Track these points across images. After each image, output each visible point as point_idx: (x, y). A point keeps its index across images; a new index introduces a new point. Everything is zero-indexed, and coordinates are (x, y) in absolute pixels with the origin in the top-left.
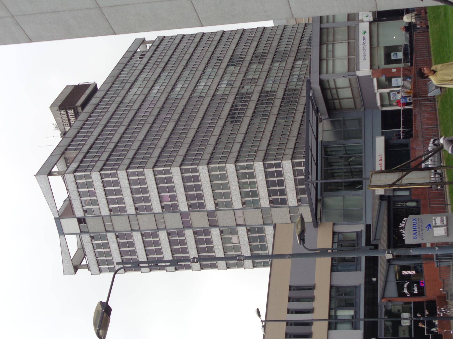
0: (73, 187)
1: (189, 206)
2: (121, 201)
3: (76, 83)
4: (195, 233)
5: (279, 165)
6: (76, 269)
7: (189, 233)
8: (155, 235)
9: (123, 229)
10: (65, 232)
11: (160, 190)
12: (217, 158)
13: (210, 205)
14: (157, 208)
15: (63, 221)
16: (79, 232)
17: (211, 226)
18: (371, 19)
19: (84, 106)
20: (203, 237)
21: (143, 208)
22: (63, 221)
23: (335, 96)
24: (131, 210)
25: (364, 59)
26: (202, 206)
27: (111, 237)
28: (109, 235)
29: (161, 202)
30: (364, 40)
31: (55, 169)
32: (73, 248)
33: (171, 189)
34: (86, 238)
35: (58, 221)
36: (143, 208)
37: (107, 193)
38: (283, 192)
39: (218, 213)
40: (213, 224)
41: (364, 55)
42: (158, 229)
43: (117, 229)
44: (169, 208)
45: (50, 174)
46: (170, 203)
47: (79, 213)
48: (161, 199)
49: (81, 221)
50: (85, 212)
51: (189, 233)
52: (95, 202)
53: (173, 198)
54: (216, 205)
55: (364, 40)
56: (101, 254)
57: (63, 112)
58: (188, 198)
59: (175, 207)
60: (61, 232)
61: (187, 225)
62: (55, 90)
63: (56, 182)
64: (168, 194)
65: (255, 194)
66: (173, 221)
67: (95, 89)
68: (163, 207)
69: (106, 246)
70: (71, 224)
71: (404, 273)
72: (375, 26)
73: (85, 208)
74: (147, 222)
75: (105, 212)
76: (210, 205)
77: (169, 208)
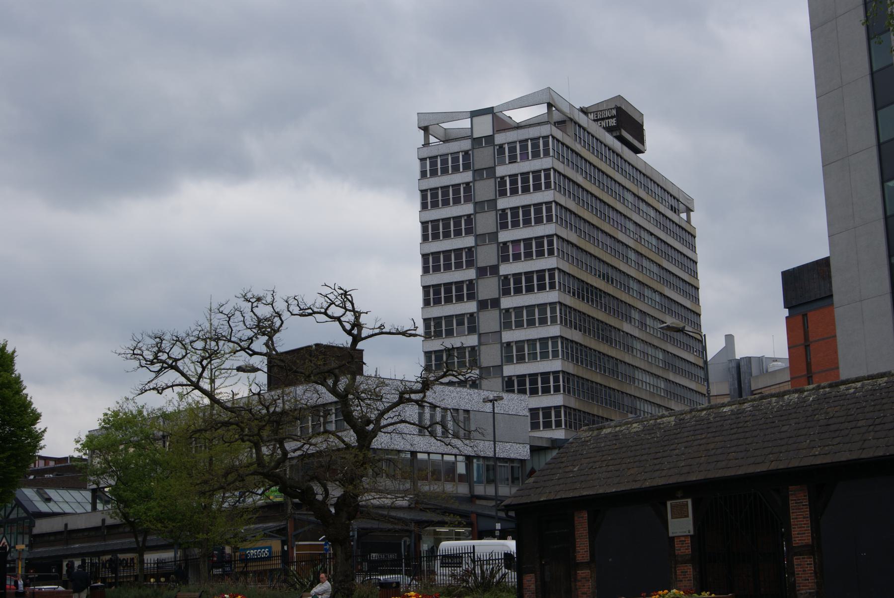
1: (506, 277)
4: (471, 281)
9: (479, 261)
10: (475, 119)
11: (527, 241)
12: (562, 247)
13: (507, 302)
15: (489, 118)
16: (475, 136)
21: (506, 219)
22: (489, 118)
24: (502, 203)
26: (506, 292)
27: (467, 176)
33: (528, 255)
34: (466, 145)
35: (490, 111)
36: (506, 219)
38: (518, 291)
40: (483, 305)
42: (480, 335)
44: (504, 252)
46: (511, 253)
47: (500, 139)
48: (516, 242)
49: (490, 139)
53: (517, 257)
58: (514, 210)
59: (505, 259)
60: (474, 114)
61: (482, 272)
64: (522, 251)
65: (521, 359)
68: (505, 243)
70: (484, 127)
73: (506, 147)
75: (501, 171)
77: (504, 252)
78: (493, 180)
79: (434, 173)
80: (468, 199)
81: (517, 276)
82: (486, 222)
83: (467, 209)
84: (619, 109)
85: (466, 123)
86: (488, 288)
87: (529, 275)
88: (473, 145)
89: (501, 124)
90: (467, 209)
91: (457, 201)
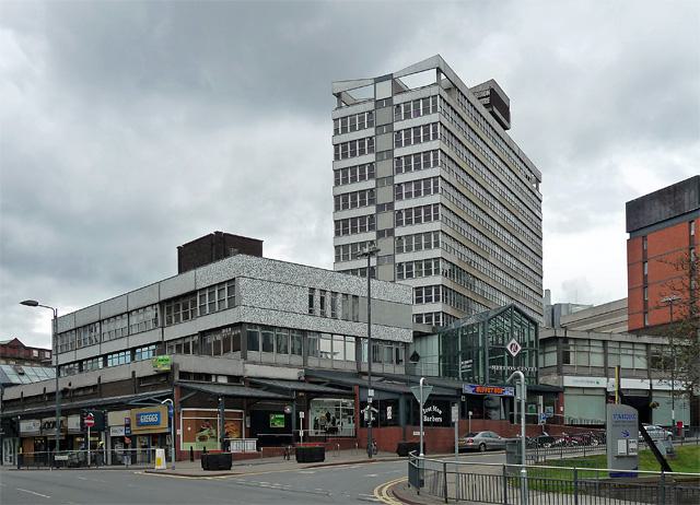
0: (425, 93)
1: (400, 212)
2: (408, 143)
3: (514, 110)
5: (437, 299)
6: (338, 95)
7: (372, 210)
8: (371, 176)
11: (417, 182)
14: (398, 179)
17: (378, 232)
19: (492, 113)
20: (369, 223)
21: (404, 164)
24: (398, 152)
26: (399, 223)
27: (371, 132)
28: (373, 129)
29: (405, 183)
31: (443, 77)
32: (358, 95)
33: (418, 194)
34: (371, 106)
35: (389, 77)
36: (404, 164)
37: (416, 129)
40: (380, 234)
41: (577, 381)
43: (379, 138)
45: (439, 71)
47: (397, 100)
49: (389, 100)
50: (398, 106)
51: (372, 210)
52: (407, 116)
53: (409, 195)
56: (353, 121)
57: (488, 93)
59: (399, 197)
60: (378, 80)
61: (380, 208)
62: (506, 88)
63: (430, 77)
66: (384, 195)
67: (506, 128)
69: (362, 127)
70: (385, 90)
71: (389, 408)
72: (602, 393)
75: (397, 126)
76: (399, 232)
79: (344, 130)
80: (371, 150)
81: (408, 211)
83: (369, 158)
84: (492, 90)
85: (368, 93)
88: (375, 106)
89: (399, 89)
90: (369, 158)
91: (362, 152)
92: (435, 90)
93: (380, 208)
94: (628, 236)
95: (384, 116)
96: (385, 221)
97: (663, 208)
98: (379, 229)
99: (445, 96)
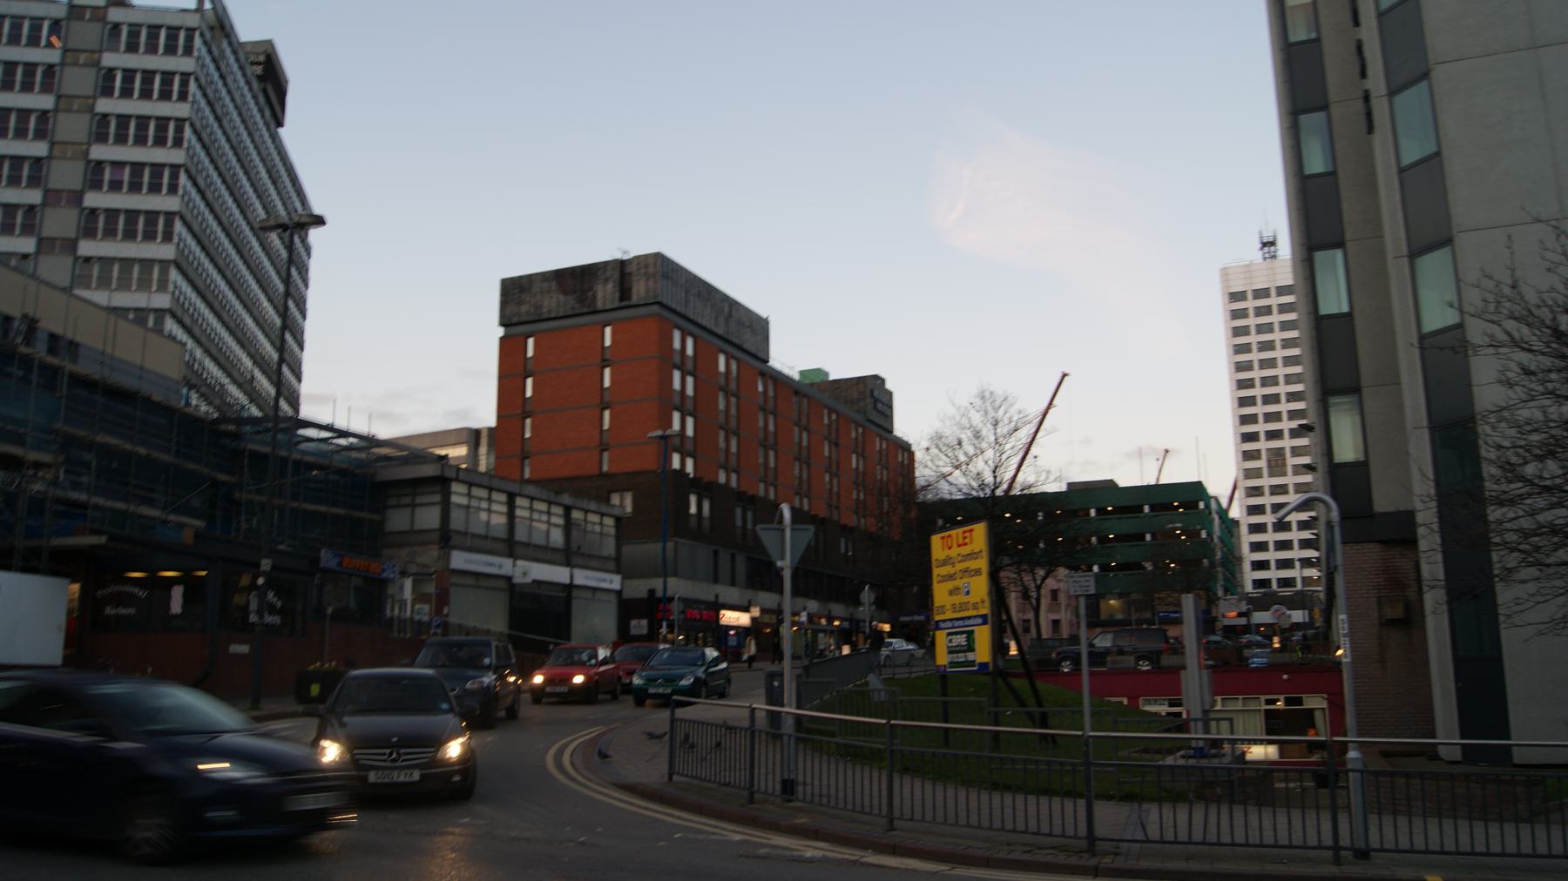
7: (34, 196)
11: (137, 167)
18: (517, 580)
23: (419, 500)
25: (466, 561)
30: (491, 564)
39: (70, 260)
40: (46, 245)
41: (471, 562)
43: (68, 71)
44: (95, 175)
51: (34, 196)
52: (132, 47)
53: (116, 186)
54: (88, 260)
55: (491, 564)
59: (96, 185)
72: (502, 584)
74: (72, 127)
77: (95, 175)
78: (94, 70)
82: (72, 127)
86: (60, 222)
87: (132, 215)
92: (193, 21)
93: (53, 197)
94: (501, 332)
95: (85, 34)
96: (60, 222)
97: (562, 297)
98: (46, 233)
99: (208, 36)
